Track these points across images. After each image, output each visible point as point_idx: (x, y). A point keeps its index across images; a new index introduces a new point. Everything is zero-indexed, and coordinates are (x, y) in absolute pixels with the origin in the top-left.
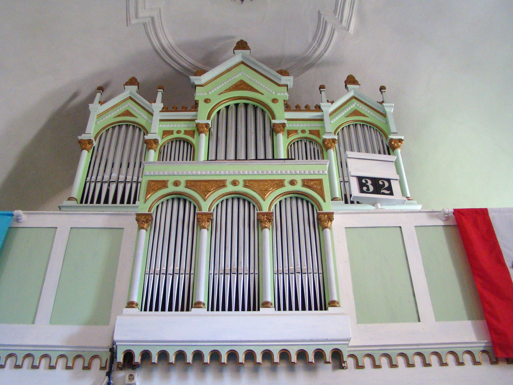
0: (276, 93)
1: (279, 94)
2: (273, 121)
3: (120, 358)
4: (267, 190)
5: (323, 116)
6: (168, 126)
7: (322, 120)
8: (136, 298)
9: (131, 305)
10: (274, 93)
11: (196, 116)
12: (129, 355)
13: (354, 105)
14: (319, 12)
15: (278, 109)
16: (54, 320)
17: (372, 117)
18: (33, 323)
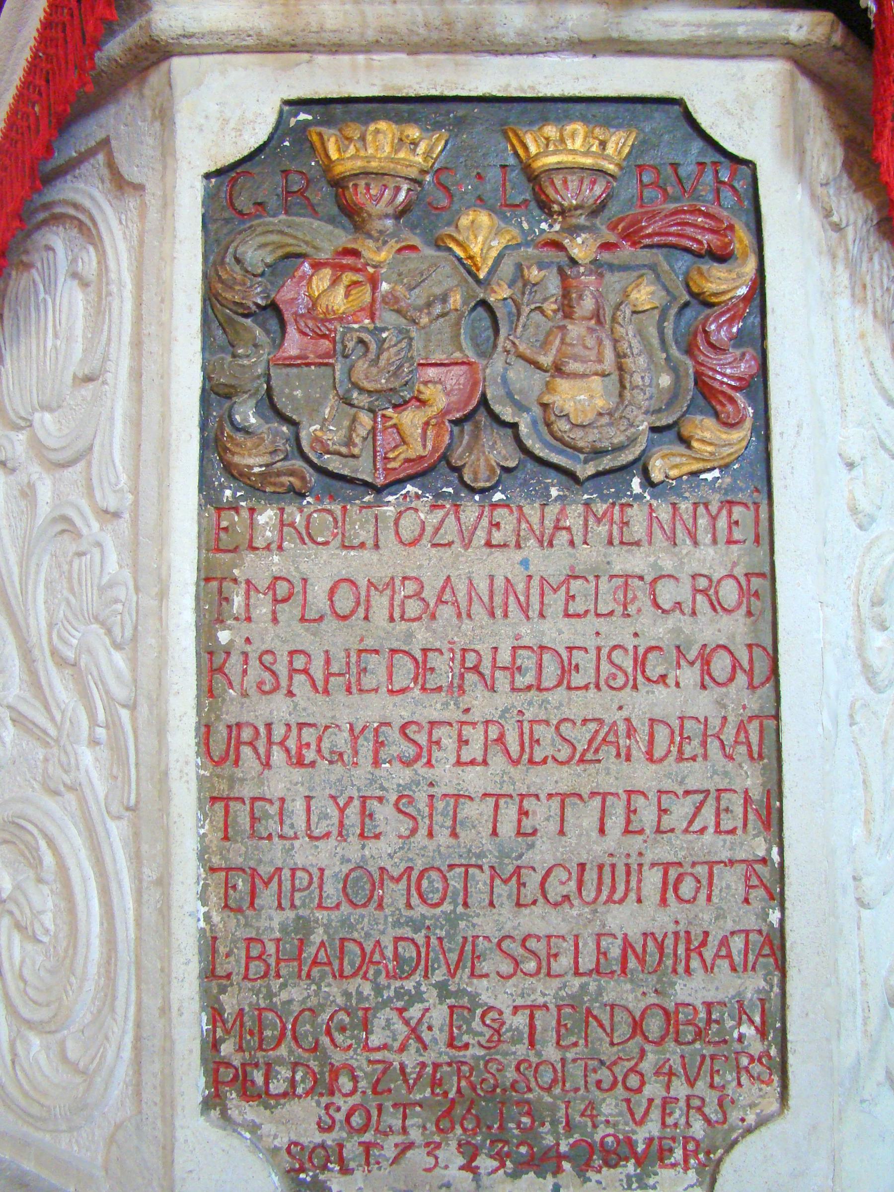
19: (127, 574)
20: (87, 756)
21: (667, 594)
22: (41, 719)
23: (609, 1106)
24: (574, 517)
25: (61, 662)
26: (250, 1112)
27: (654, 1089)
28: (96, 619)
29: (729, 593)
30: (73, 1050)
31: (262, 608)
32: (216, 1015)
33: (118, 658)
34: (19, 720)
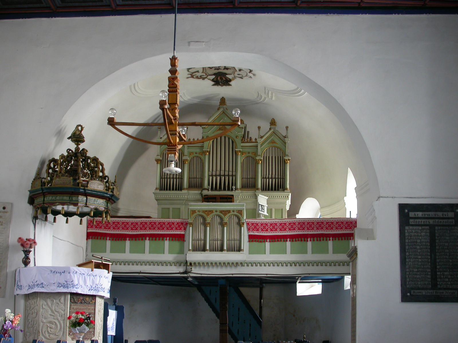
0: (238, 133)
1: (239, 133)
2: (236, 150)
3: (189, 264)
4: (226, 214)
5: (257, 145)
6: (192, 150)
7: (257, 146)
8: (191, 248)
9: (189, 250)
10: (237, 132)
11: (203, 145)
12: (191, 264)
13: (272, 137)
14: (258, 92)
15: (238, 141)
16: (170, 252)
17: (279, 143)
18: (164, 253)
19: (64, 307)
20: (59, 317)
21: (90, 309)
22: (54, 315)
23: (86, 336)
24: (87, 305)
25: (56, 311)
26: (70, 336)
27: (88, 335)
28: (61, 309)
29: (93, 309)
30: (57, 334)
31: (72, 309)
32: (69, 330)
33: (63, 311)
34: (50, 315)
